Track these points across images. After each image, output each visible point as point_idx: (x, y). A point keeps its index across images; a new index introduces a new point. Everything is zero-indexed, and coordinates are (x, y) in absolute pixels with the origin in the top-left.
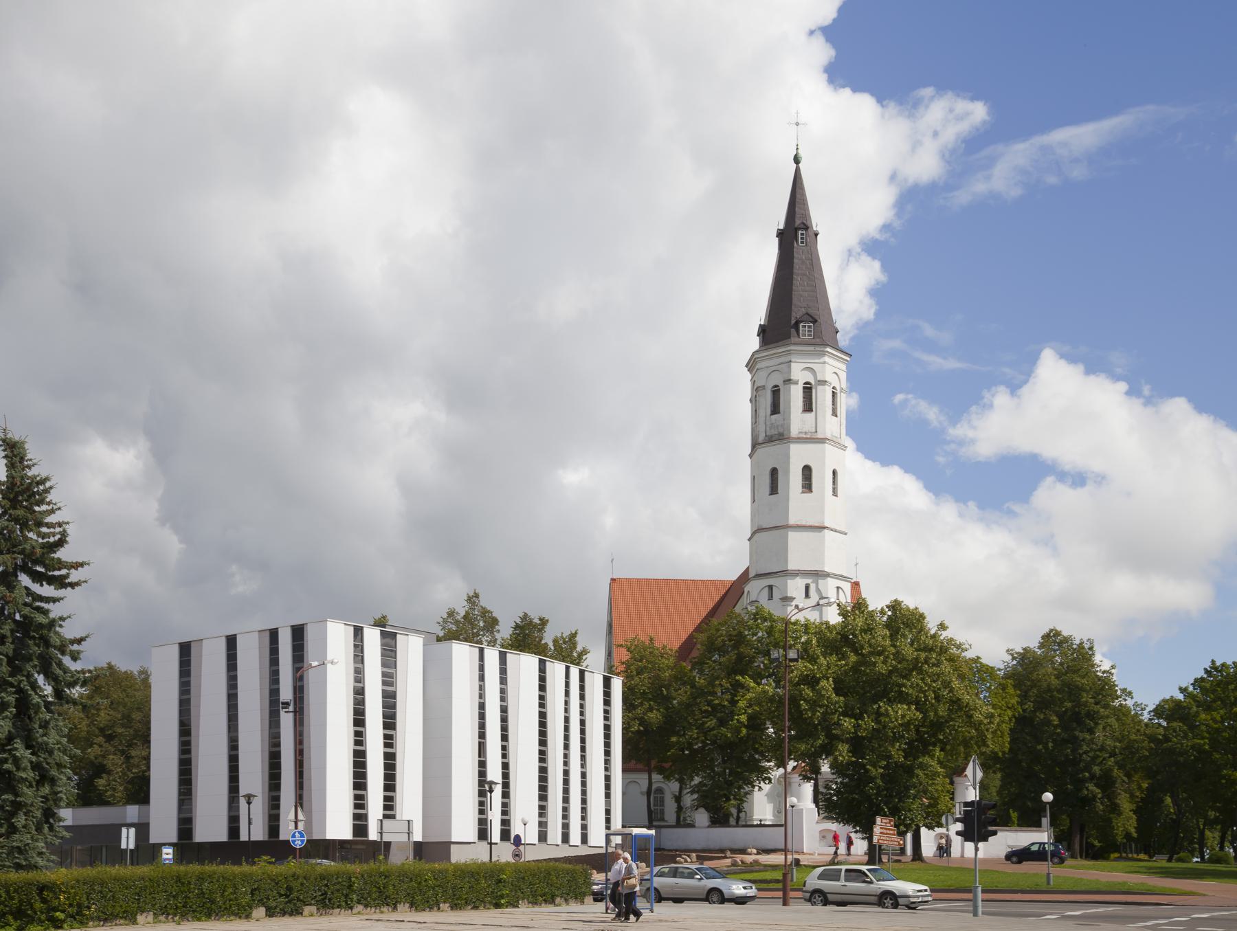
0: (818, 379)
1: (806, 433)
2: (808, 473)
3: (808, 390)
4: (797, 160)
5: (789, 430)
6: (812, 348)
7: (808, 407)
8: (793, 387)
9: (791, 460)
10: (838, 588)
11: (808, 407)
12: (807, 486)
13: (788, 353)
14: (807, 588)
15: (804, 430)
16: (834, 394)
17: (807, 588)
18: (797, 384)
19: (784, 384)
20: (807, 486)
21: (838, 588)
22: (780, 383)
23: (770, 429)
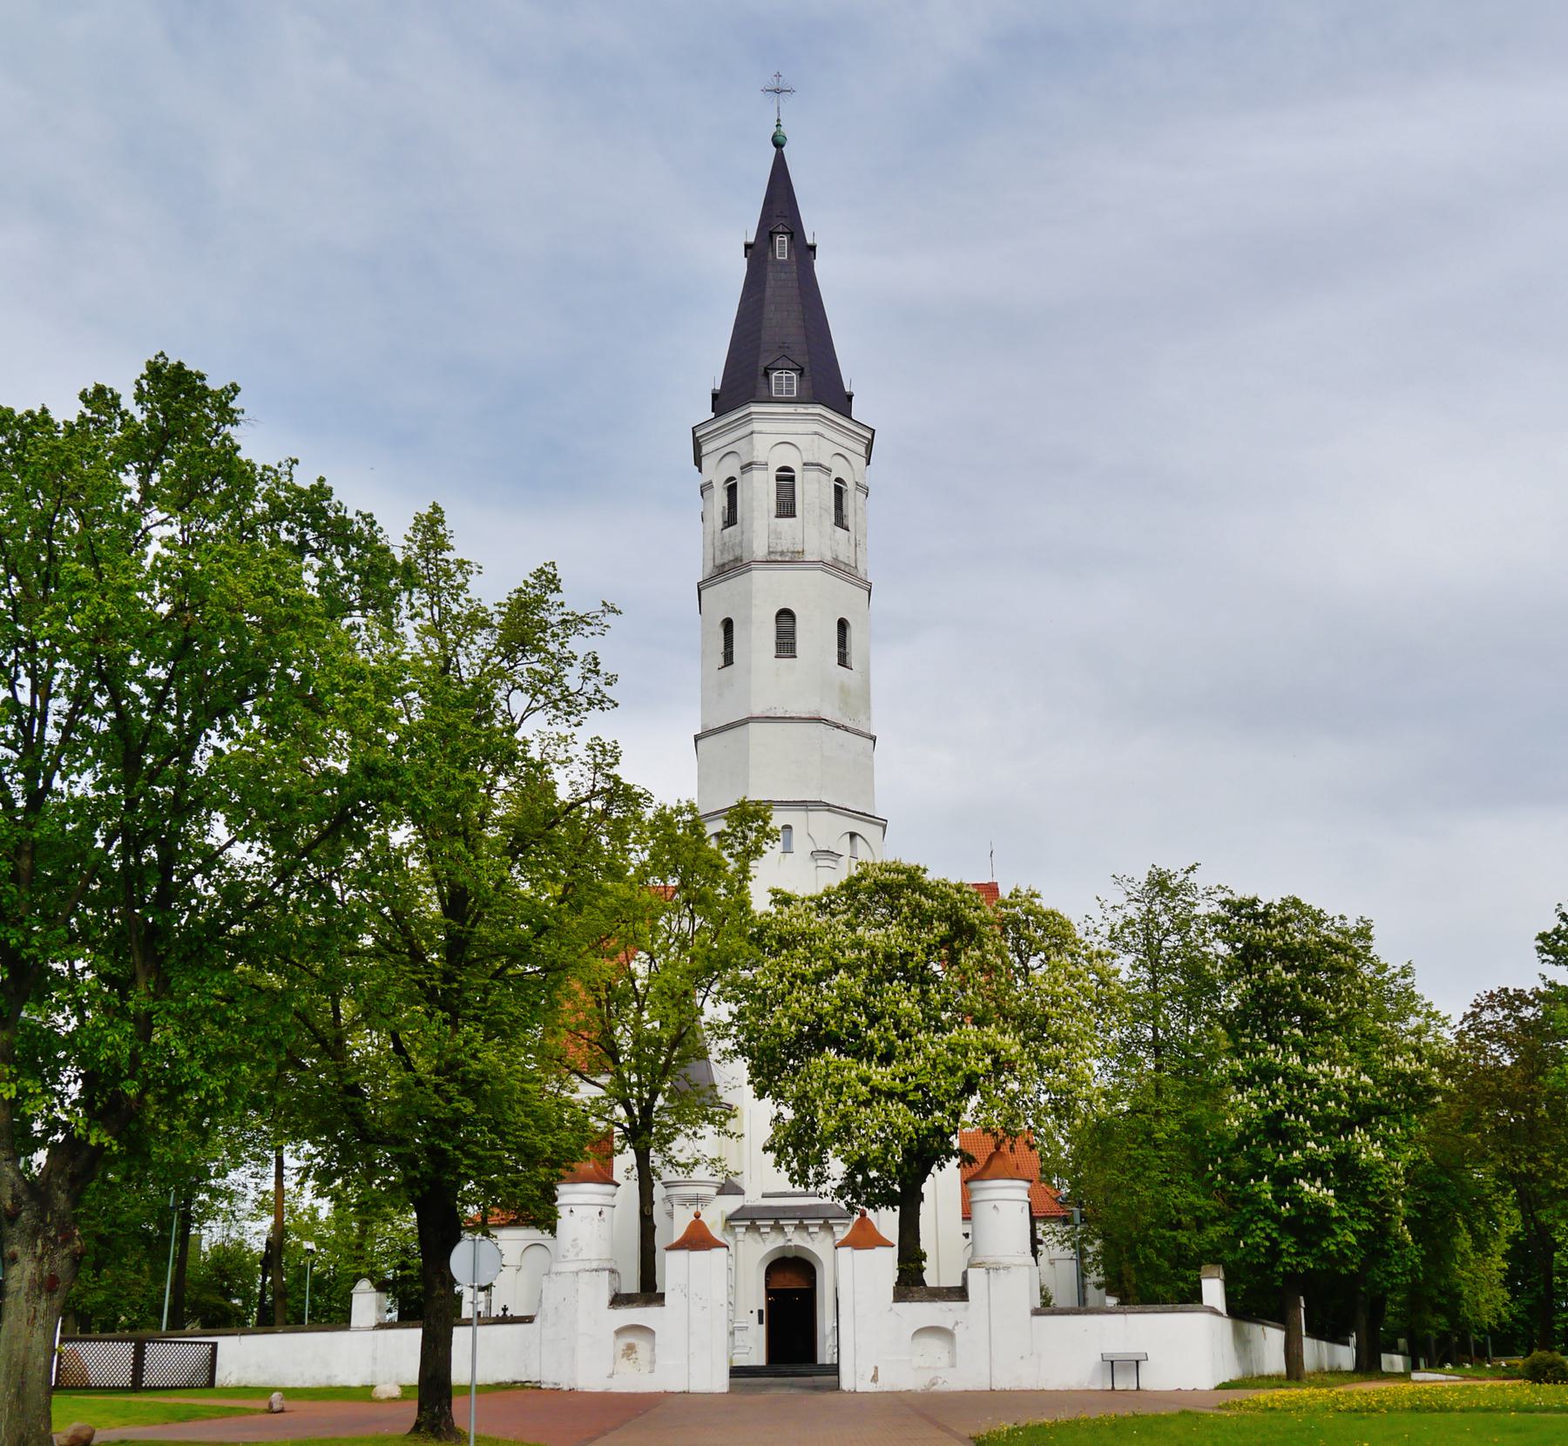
1: (782, 553)
2: (786, 624)
3: (786, 477)
4: (778, 144)
6: (790, 409)
7: (786, 508)
8: (756, 474)
10: (853, 835)
11: (786, 508)
12: (786, 644)
15: (779, 549)
16: (839, 492)
19: (743, 473)
20: (786, 644)
21: (853, 835)
22: (736, 472)
23: (722, 553)
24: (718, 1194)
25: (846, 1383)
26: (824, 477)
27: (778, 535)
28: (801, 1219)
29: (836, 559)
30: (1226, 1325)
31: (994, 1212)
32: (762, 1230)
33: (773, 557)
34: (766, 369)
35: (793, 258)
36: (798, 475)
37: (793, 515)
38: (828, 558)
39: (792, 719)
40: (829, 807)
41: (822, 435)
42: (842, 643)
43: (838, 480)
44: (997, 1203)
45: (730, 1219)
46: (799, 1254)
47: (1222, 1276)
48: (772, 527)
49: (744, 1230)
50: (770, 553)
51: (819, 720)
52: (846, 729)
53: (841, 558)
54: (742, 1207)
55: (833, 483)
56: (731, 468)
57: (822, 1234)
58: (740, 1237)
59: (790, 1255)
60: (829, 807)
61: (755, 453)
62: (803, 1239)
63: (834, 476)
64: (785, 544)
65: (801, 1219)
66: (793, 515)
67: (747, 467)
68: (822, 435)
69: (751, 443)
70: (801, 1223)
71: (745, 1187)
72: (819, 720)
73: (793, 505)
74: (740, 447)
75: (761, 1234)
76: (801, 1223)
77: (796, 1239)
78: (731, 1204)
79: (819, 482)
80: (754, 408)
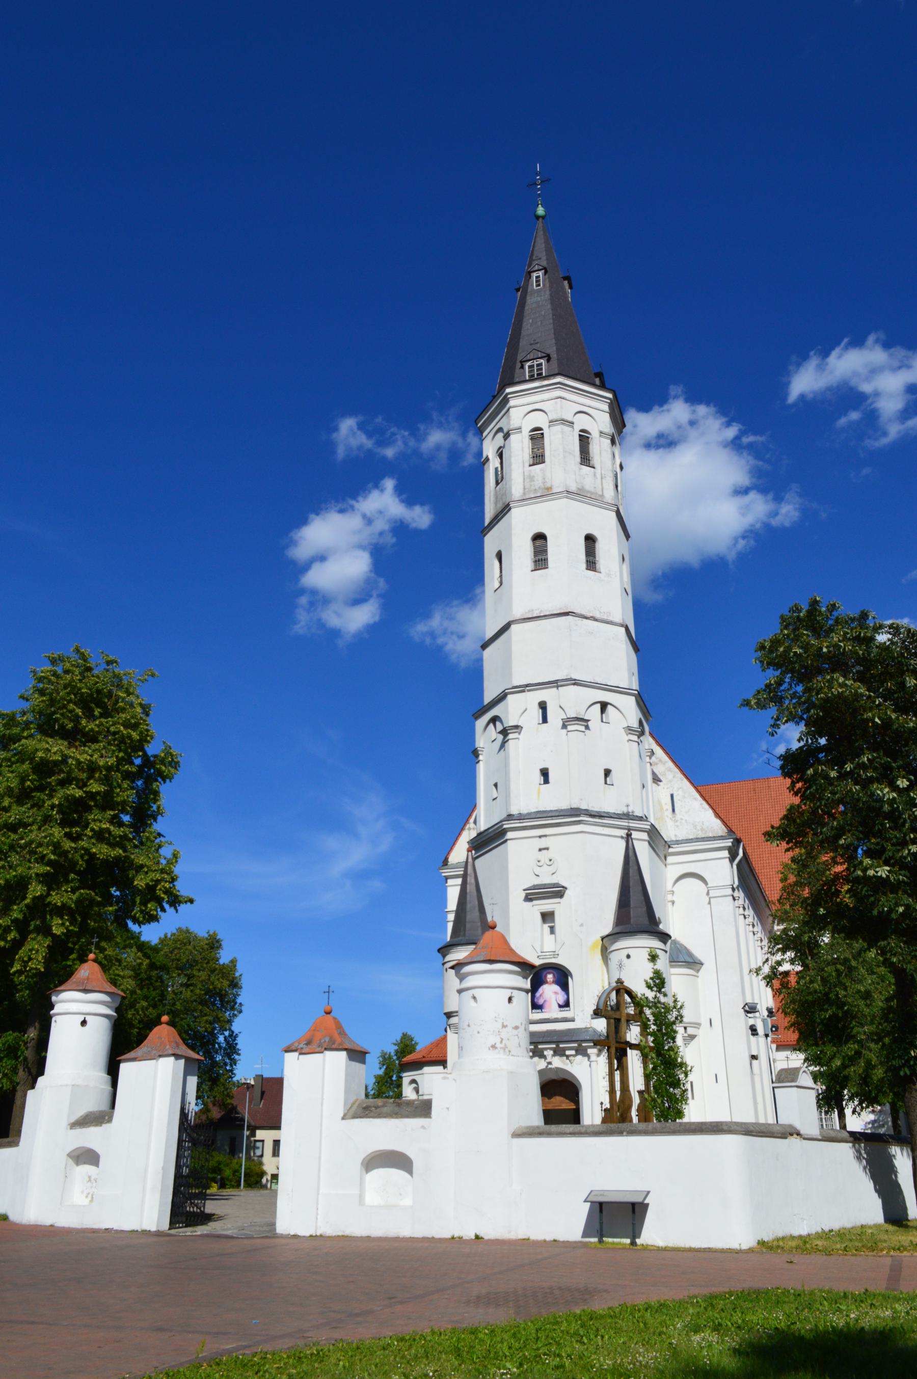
0: (551, 418)
2: (539, 543)
3: (537, 436)
5: (511, 492)
7: (538, 458)
9: (514, 532)
10: (604, 706)
11: (538, 458)
12: (540, 560)
13: (506, 401)
14: (543, 706)
15: (533, 488)
17: (543, 706)
20: (540, 560)
26: (567, 429)
27: (532, 479)
28: (557, 1043)
33: (527, 497)
36: (546, 432)
38: (573, 488)
39: (546, 617)
40: (576, 683)
41: (563, 398)
43: (582, 431)
48: (526, 474)
50: (524, 494)
51: (566, 614)
52: (596, 620)
53: (587, 488)
57: (579, 1057)
60: (576, 683)
61: (512, 422)
62: (563, 1062)
63: (578, 428)
64: (538, 483)
65: (557, 1043)
67: (507, 436)
68: (563, 398)
70: (580, 1045)
72: (566, 614)
73: (543, 456)
76: (580, 1045)
77: (558, 1062)
80: (508, 390)
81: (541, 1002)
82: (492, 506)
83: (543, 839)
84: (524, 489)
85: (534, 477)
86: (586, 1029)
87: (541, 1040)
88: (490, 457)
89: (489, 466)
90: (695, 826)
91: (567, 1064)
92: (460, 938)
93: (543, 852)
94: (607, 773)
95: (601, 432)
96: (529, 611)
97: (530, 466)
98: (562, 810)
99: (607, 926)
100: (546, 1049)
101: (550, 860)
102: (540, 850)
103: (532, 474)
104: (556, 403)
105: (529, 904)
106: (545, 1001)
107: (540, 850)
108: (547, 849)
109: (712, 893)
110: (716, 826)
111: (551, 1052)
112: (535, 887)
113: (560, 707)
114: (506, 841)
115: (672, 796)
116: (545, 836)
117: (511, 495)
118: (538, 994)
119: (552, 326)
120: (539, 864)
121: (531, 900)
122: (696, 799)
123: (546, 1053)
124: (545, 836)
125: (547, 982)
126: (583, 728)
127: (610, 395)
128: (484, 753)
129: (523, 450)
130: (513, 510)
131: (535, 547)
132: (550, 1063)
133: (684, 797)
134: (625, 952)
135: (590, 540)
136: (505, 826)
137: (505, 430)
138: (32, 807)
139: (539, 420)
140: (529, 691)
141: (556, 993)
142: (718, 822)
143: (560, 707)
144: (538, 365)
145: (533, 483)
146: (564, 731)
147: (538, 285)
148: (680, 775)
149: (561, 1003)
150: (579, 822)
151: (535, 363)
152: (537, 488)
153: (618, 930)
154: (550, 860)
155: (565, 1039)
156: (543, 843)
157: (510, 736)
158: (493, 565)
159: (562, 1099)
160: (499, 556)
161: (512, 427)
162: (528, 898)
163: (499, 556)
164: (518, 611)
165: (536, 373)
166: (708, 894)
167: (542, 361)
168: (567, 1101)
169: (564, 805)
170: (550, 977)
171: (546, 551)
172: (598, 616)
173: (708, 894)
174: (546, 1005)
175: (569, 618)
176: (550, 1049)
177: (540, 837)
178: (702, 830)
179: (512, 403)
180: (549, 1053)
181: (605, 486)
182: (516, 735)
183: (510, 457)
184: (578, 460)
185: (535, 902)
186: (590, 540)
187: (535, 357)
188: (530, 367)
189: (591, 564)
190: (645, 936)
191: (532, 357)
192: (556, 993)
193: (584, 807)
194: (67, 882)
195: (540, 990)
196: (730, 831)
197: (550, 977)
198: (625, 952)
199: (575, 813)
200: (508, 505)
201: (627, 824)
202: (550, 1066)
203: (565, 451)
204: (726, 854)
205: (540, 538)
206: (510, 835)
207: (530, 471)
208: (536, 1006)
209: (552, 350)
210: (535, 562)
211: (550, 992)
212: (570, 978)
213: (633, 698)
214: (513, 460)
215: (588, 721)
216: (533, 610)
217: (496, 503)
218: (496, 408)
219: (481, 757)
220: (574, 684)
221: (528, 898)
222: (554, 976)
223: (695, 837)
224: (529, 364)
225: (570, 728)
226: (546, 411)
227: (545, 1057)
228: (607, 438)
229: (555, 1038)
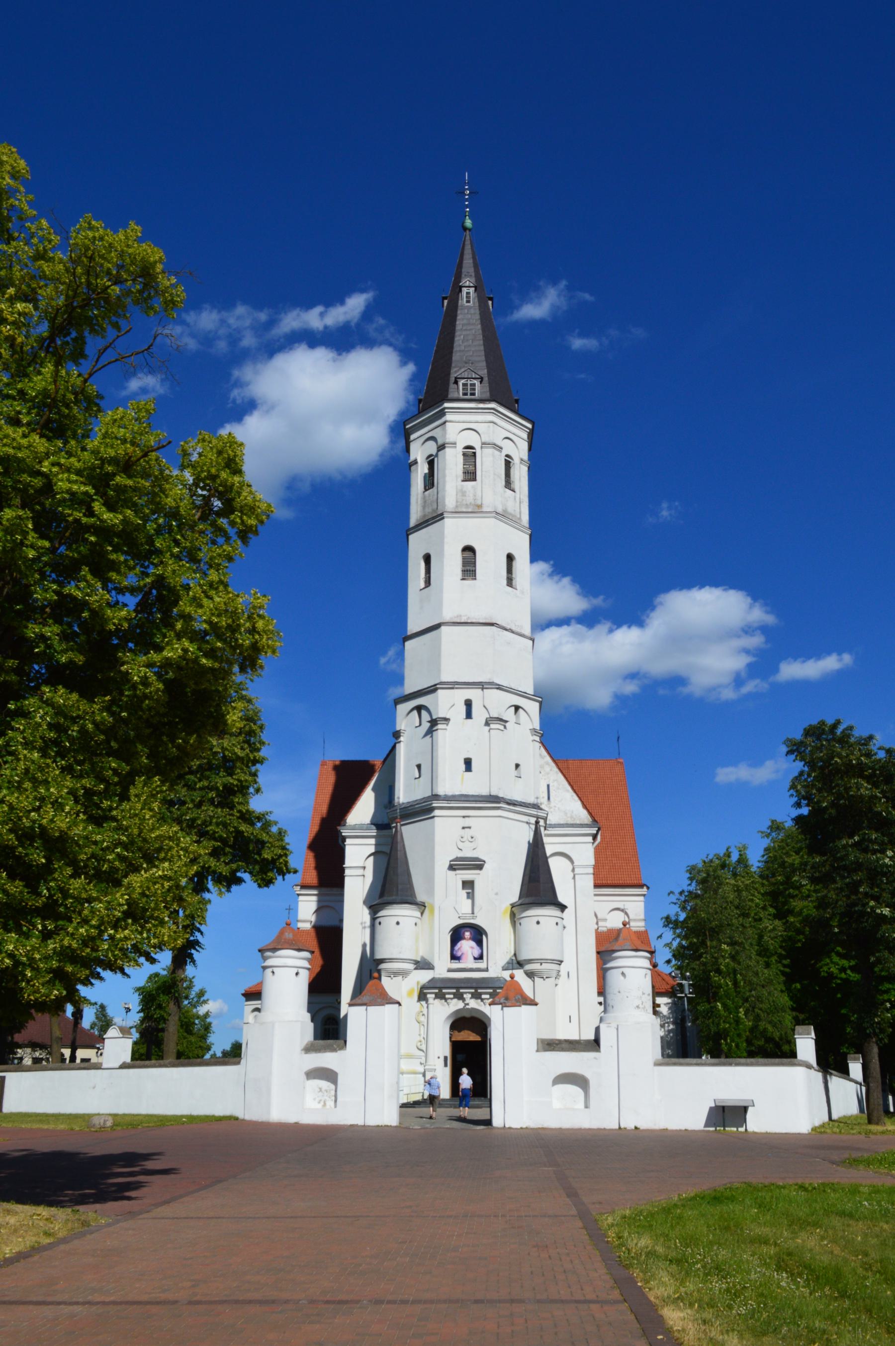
0: (484, 440)
2: (468, 554)
3: (470, 454)
5: (444, 502)
7: (470, 475)
9: (446, 540)
10: (517, 708)
11: (470, 475)
13: (442, 413)
14: (468, 704)
15: (464, 502)
16: (508, 465)
17: (468, 704)
18: (455, 447)
21: (517, 708)
24: (416, 969)
25: (497, 1122)
26: (497, 453)
27: (463, 493)
28: (476, 988)
29: (505, 511)
30: (820, 1075)
31: (622, 978)
32: (447, 996)
33: (460, 510)
34: (456, 378)
35: (477, 304)
37: (475, 479)
38: (500, 510)
40: (499, 687)
42: (510, 570)
43: (507, 456)
44: (625, 970)
45: (423, 988)
46: (474, 1015)
47: (813, 1035)
49: (433, 996)
50: (457, 506)
51: (492, 624)
52: (513, 632)
53: (510, 510)
54: (433, 980)
55: (503, 458)
56: (431, 447)
58: (431, 1001)
59: (467, 1015)
60: (499, 687)
61: (447, 436)
62: (477, 1003)
63: (504, 452)
64: (470, 499)
65: (476, 988)
66: (475, 479)
67: (441, 448)
69: (444, 430)
70: (476, 991)
71: (436, 963)
72: (492, 624)
73: (474, 473)
74: (436, 433)
75: (446, 999)
76: (476, 991)
77: (473, 1004)
78: (424, 976)
79: (493, 456)
80: (446, 405)
81: (459, 954)
82: (420, 508)
83: (467, 819)
84: (457, 502)
85: (465, 492)
86: (497, 979)
87: (463, 985)
88: (419, 461)
89: (417, 469)
90: (566, 814)
91: (481, 1006)
92: (394, 897)
93: (466, 829)
94: (517, 766)
95: (522, 460)
96: (457, 616)
97: (463, 481)
98: (482, 796)
99: (514, 897)
100: (466, 993)
101: (472, 838)
102: (463, 828)
103: (464, 489)
104: (489, 427)
105: (452, 873)
106: (462, 954)
107: (463, 828)
108: (470, 828)
109: (577, 871)
110: (583, 815)
111: (470, 996)
112: (457, 859)
113: (484, 706)
114: (433, 817)
115: (548, 786)
116: (468, 817)
117: (444, 505)
118: (456, 948)
119: (482, 348)
120: (462, 840)
121: (455, 870)
122: (568, 791)
123: (465, 996)
124: (468, 817)
125: (464, 938)
126: (502, 727)
127: (530, 426)
128: (405, 735)
129: (456, 465)
130: (446, 520)
131: (464, 558)
132: (468, 1004)
133: (558, 788)
134: (536, 919)
135: (510, 558)
136: (434, 805)
137: (440, 442)
138: (184, 786)
139: (473, 440)
140: (457, 688)
141: (472, 948)
142: (585, 812)
143: (484, 706)
144: (471, 385)
145: (464, 498)
146: (487, 728)
147: (468, 302)
148: (555, 769)
149: (476, 956)
150: (498, 808)
151: (469, 382)
152: (468, 503)
153: (527, 900)
154: (472, 838)
155: (483, 985)
156: (467, 822)
157: (439, 726)
158: (419, 564)
159: (470, 1032)
160: (427, 559)
161: (447, 441)
162: (452, 868)
163: (427, 559)
164: (448, 615)
165: (469, 392)
166: (573, 870)
167: (475, 381)
168: (474, 1034)
169: (484, 792)
170: (467, 934)
171: (475, 563)
172: (514, 629)
173: (573, 870)
174: (463, 957)
175: (493, 628)
176: (469, 993)
177: (464, 817)
178: (572, 817)
179: (448, 417)
180: (467, 996)
181: (522, 510)
182: (443, 726)
183: (444, 469)
184: (503, 483)
185: (458, 872)
186: (510, 558)
187: (470, 376)
188: (464, 385)
189: (510, 582)
190: (552, 907)
191: (466, 376)
192: (472, 948)
193: (501, 795)
194: (225, 854)
195: (459, 945)
196: (595, 821)
197: (467, 934)
198: (536, 919)
199: (493, 800)
200: (442, 514)
201: (535, 813)
202: (467, 1007)
203: (495, 474)
204: (590, 839)
205: (469, 550)
206: (437, 812)
207: (462, 486)
208: (454, 957)
209: (484, 372)
210: (463, 571)
211: (467, 946)
212: (484, 937)
213: (537, 704)
214: (447, 472)
215: (506, 722)
216: (461, 616)
217: (424, 507)
218: (429, 417)
219: (402, 739)
220: (497, 688)
221: (452, 868)
222: (471, 933)
223: (565, 822)
224: (463, 381)
225: (492, 726)
226: (480, 432)
227: (463, 1000)
228: (525, 465)
229: (474, 985)
